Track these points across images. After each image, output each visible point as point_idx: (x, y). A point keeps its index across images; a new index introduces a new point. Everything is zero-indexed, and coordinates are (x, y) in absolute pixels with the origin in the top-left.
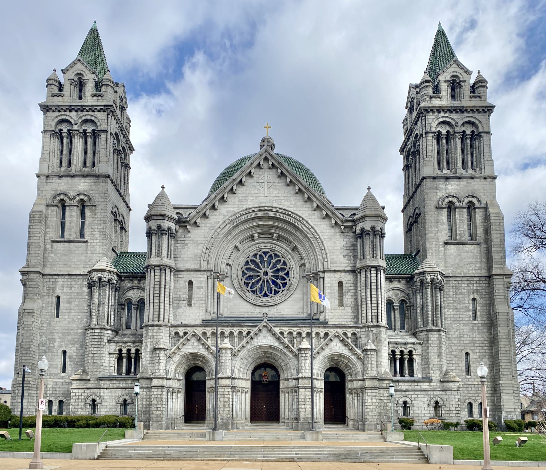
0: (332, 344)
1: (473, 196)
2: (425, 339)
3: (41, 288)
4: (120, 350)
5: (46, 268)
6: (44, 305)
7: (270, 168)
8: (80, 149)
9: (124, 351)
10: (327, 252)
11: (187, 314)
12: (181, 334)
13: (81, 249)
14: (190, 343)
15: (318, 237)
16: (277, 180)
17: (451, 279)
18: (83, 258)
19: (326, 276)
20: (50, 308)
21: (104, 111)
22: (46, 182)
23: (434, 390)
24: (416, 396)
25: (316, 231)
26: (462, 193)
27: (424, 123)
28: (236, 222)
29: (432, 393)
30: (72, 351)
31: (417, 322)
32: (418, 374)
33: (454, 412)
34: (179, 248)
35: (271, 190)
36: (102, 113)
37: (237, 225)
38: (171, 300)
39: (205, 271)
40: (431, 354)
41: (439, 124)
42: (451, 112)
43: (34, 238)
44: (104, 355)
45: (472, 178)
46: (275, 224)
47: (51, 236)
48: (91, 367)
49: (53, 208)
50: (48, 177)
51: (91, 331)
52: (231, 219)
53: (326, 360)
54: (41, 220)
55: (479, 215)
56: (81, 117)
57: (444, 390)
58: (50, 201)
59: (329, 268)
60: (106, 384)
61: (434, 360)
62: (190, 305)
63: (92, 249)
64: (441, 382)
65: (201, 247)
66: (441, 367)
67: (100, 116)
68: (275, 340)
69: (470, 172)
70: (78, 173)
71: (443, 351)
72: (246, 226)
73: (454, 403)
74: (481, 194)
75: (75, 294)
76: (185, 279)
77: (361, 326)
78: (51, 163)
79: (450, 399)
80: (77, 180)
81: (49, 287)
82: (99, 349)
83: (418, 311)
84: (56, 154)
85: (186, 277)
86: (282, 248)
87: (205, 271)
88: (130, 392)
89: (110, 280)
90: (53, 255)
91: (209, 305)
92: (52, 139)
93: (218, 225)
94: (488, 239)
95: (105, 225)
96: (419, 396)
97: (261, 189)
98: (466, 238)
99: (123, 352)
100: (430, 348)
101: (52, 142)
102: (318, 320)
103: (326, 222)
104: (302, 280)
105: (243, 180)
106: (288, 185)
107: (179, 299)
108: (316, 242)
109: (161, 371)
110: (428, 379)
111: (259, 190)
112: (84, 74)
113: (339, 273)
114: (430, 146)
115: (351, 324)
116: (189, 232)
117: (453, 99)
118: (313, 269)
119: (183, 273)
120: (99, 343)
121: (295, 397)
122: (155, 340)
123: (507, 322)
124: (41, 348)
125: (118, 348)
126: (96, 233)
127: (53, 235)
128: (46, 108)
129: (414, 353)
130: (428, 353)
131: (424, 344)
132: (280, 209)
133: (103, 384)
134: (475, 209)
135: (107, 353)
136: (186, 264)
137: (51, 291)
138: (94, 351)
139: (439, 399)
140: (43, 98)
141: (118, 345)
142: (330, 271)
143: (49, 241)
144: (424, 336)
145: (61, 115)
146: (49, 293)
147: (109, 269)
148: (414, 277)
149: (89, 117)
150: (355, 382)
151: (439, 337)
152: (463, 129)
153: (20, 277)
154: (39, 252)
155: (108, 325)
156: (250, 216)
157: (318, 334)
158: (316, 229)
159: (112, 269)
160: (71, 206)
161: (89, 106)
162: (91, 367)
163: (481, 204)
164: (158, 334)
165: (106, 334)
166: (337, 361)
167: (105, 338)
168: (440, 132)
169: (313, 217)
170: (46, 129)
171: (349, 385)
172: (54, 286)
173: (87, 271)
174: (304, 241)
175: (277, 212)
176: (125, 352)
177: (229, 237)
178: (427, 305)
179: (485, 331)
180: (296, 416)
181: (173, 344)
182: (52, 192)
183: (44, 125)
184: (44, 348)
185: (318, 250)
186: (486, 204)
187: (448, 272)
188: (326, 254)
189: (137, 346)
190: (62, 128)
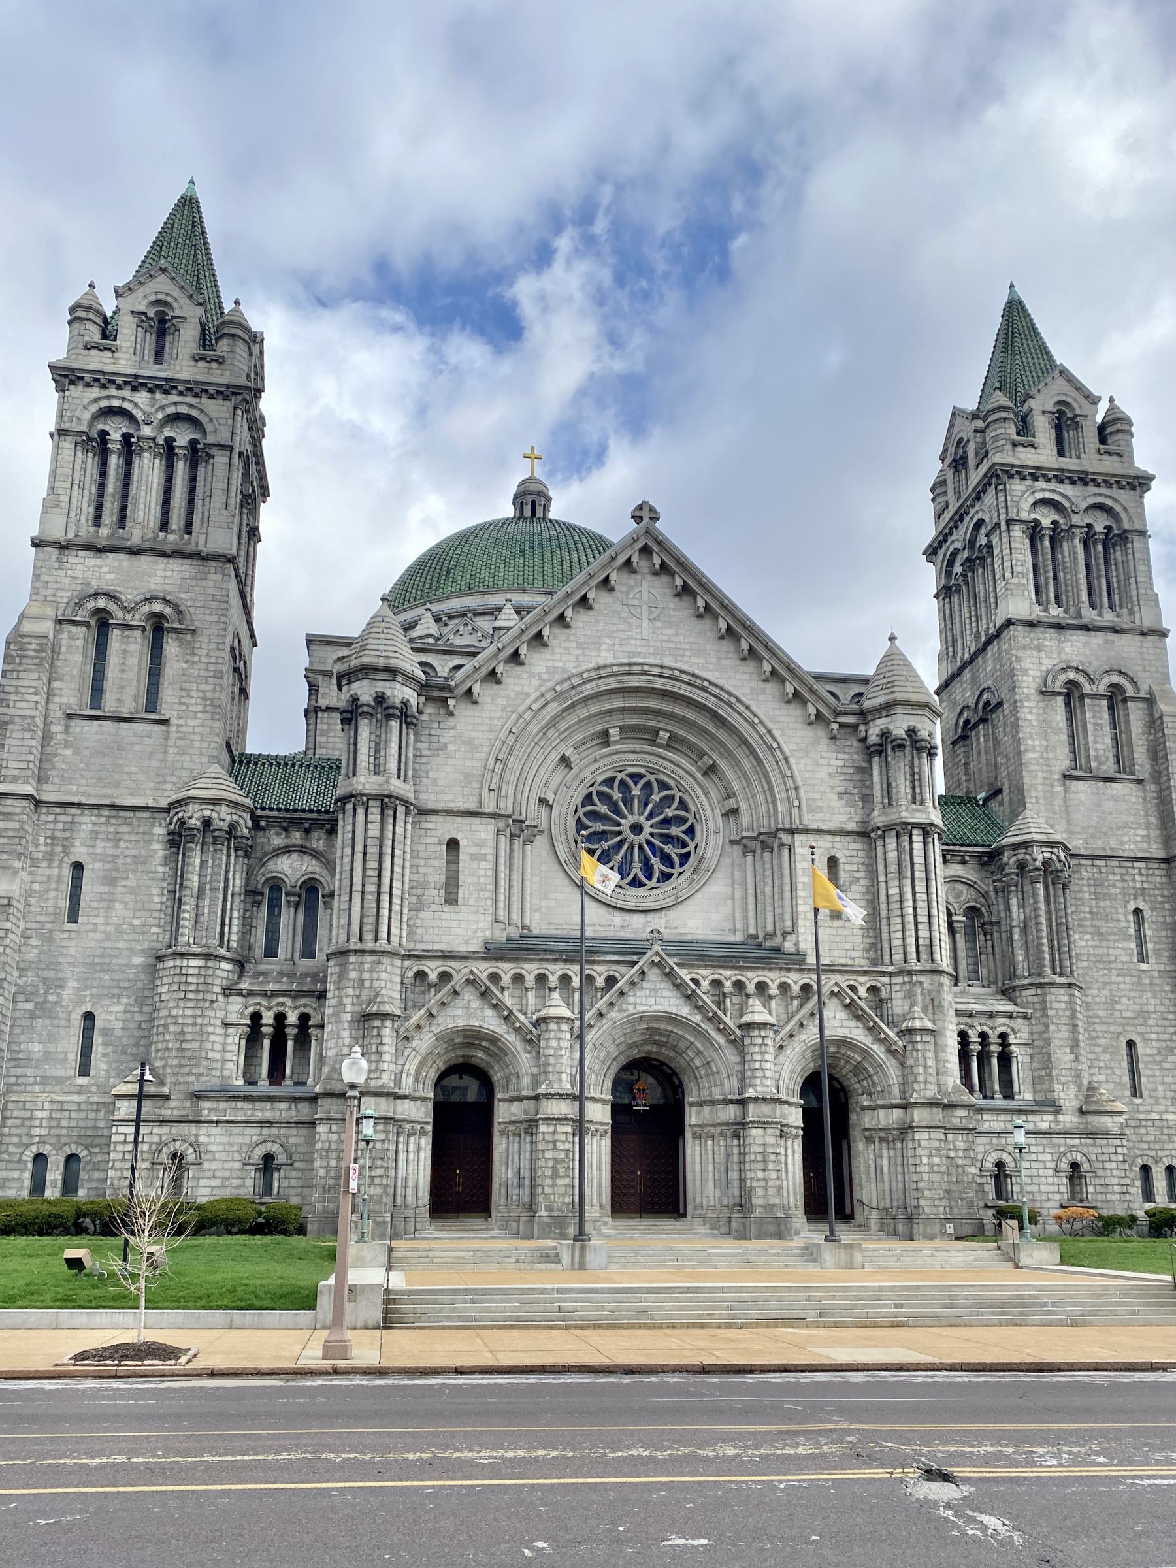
1: (1121, 672)
2: (1038, 1006)
3: (30, 838)
4: (256, 1017)
5: (45, 787)
6: (36, 887)
7: (655, 574)
8: (155, 486)
9: (268, 1018)
10: (800, 783)
12: (433, 977)
13: (150, 741)
14: (459, 1002)
15: (775, 745)
16: (673, 603)
17: (1083, 862)
18: (155, 764)
20: (52, 894)
21: (226, 398)
22: (59, 560)
25: (769, 732)
26: (1095, 663)
27: (1002, 499)
28: (571, 697)
30: (111, 1016)
31: (1013, 965)
32: (1024, 1094)
34: (425, 752)
35: (658, 624)
36: (220, 402)
38: (406, 886)
39: (494, 815)
40: (1055, 1043)
41: (1035, 504)
42: (1061, 482)
43: (19, 705)
44: (210, 1029)
45: (1115, 631)
46: (666, 707)
47: (65, 700)
48: (175, 1062)
49: (74, 629)
50: (64, 547)
51: (178, 962)
52: (558, 688)
53: (809, 1054)
54: (42, 659)
55: (1136, 715)
56: (162, 408)
58: (69, 611)
59: (805, 822)
60: (216, 1110)
61: (1062, 1057)
62: (451, 900)
63: (181, 743)
65: (484, 756)
67: (215, 410)
68: (681, 1001)
69: (1109, 617)
70: (147, 545)
72: (595, 708)
74: (1137, 668)
75: (129, 860)
76: (439, 833)
77: (891, 969)
78: (72, 514)
80: (144, 560)
81: (53, 838)
82: (199, 1012)
83: (1016, 937)
84: (86, 492)
85: (440, 829)
86: (678, 769)
87: (494, 815)
88: (283, 1131)
89: (233, 826)
90: (68, 752)
91: (501, 904)
92: (79, 454)
93: (528, 702)
94: (1160, 772)
95: (218, 681)
97: (634, 621)
98: (1109, 767)
99: (264, 1021)
100: (1052, 1027)
101: (79, 461)
102: (778, 950)
103: (794, 711)
104: (728, 848)
105: (591, 596)
106: (700, 616)
107: (423, 885)
108: (771, 758)
109: (385, 1076)
111: (630, 624)
112: (175, 305)
113: (829, 837)
114: (1015, 555)
115: (864, 964)
116: (451, 714)
117: (1061, 453)
118: (764, 825)
119: (433, 818)
120: (200, 996)
121: (735, 1151)
122: (366, 992)
124: (20, 1006)
125: (251, 1009)
126: (193, 701)
127: (72, 700)
129: (1012, 1039)
130: (1048, 1042)
131: (1037, 1016)
132: (682, 672)
133: (207, 1109)
134: (1125, 700)
135: (218, 1022)
136: (440, 796)
137: (59, 849)
138: (184, 1016)
140: (59, 352)
141: (252, 1001)
142: (807, 831)
143: (59, 714)
144: (1035, 999)
145: (109, 397)
146: (52, 854)
147: (233, 797)
148: (1002, 853)
149: (183, 410)
150: (882, 1112)
152: (1088, 520)
154: (33, 743)
155: (221, 945)
156: (606, 684)
157: (784, 987)
158: (770, 725)
159: (240, 799)
160: (125, 627)
161: (189, 382)
162: (175, 1062)
163: (1138, 690)
164: (375, 975)
165: (218, 972)
166: (832, 1056)
167: (218, 981)
168: (1037, 522)
169: (761, 697)
170: (66, 426)
171: (866, 1120)
172: (68, 834)
173: (170, 800)
174: (740, 753)
175: (675, 679)
176: (271, 1021)
178: (1038, 924)
179: (1168, 988)
180: (738, 1200)
181: (410, 1004)
182: (74, 587)
183: (60, 416)
184: (29, 1006)
185: (774, 777)
186: (1150, 692)
187: (1077, 844)
188: (797, 788)
189: (305, 1006)
190: (107, 428)
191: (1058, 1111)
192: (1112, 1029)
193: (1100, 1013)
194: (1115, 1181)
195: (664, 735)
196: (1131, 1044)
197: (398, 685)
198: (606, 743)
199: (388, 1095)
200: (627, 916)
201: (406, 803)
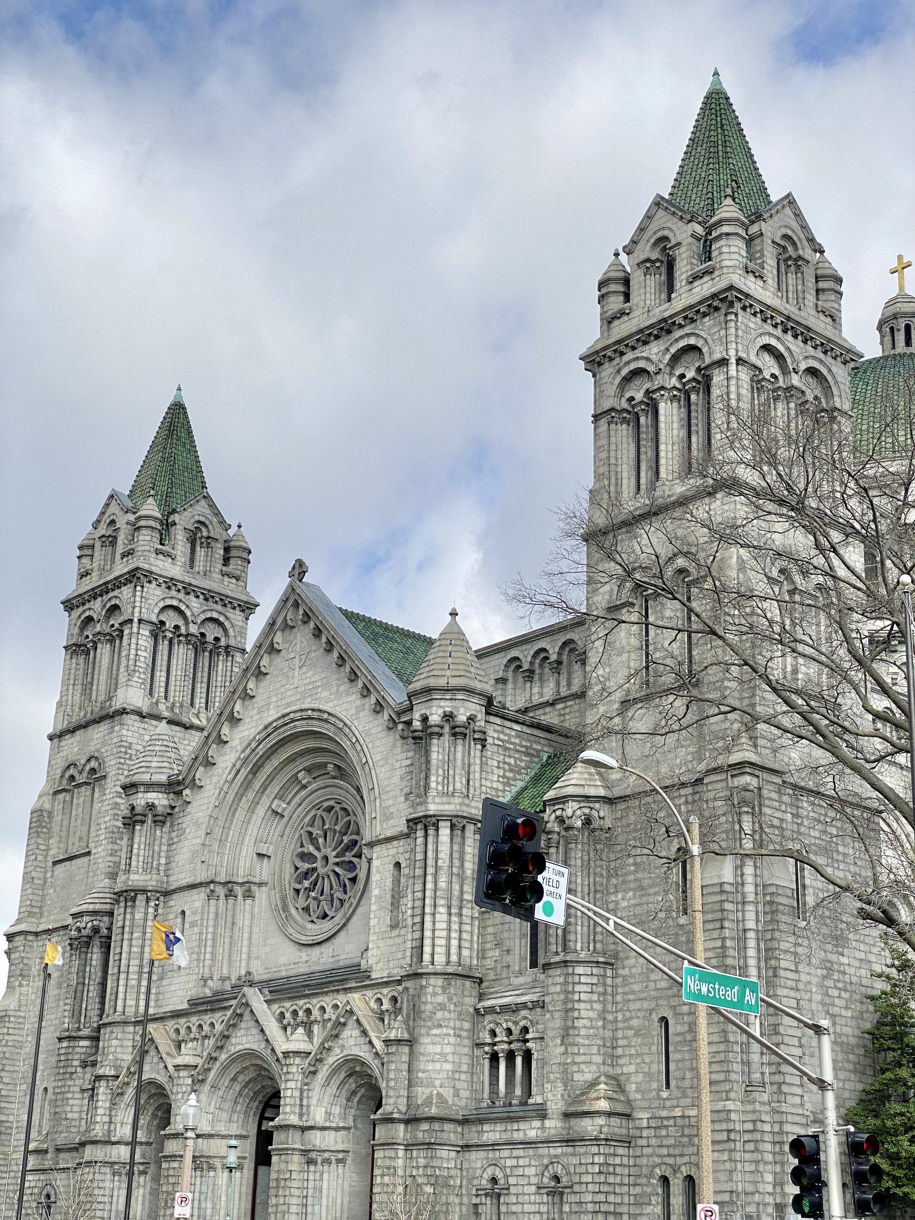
5: (43, 920)
11: (173, 988)
19: (375, 856)
29: (546, 1151)
35: (304, 669)
37: (256, 770)
39: (201, 884)
57: (568, 1141)
66: (565, 1072)
71: (579, 1023)
72: (276, 761)
73: (589, 1178)
79: (583, 1169)
85: (178, 902)
89: (96, 930)
97: (290, 674)
119: (175, 896)
132: (313, 710)
139: (559, 1170)
142: (380, 842)
151: (566, 982)
153: (5, 945)
167: (77, 1057)
175: (310, 718)
177: (251, 795)
192: (646, 1005)
193: (636, 987)
195: (330, 767)
196: (664, 1021)
197: (140, 795)
198: (304, 787)
200: (309, 951)
201: (145, 891)
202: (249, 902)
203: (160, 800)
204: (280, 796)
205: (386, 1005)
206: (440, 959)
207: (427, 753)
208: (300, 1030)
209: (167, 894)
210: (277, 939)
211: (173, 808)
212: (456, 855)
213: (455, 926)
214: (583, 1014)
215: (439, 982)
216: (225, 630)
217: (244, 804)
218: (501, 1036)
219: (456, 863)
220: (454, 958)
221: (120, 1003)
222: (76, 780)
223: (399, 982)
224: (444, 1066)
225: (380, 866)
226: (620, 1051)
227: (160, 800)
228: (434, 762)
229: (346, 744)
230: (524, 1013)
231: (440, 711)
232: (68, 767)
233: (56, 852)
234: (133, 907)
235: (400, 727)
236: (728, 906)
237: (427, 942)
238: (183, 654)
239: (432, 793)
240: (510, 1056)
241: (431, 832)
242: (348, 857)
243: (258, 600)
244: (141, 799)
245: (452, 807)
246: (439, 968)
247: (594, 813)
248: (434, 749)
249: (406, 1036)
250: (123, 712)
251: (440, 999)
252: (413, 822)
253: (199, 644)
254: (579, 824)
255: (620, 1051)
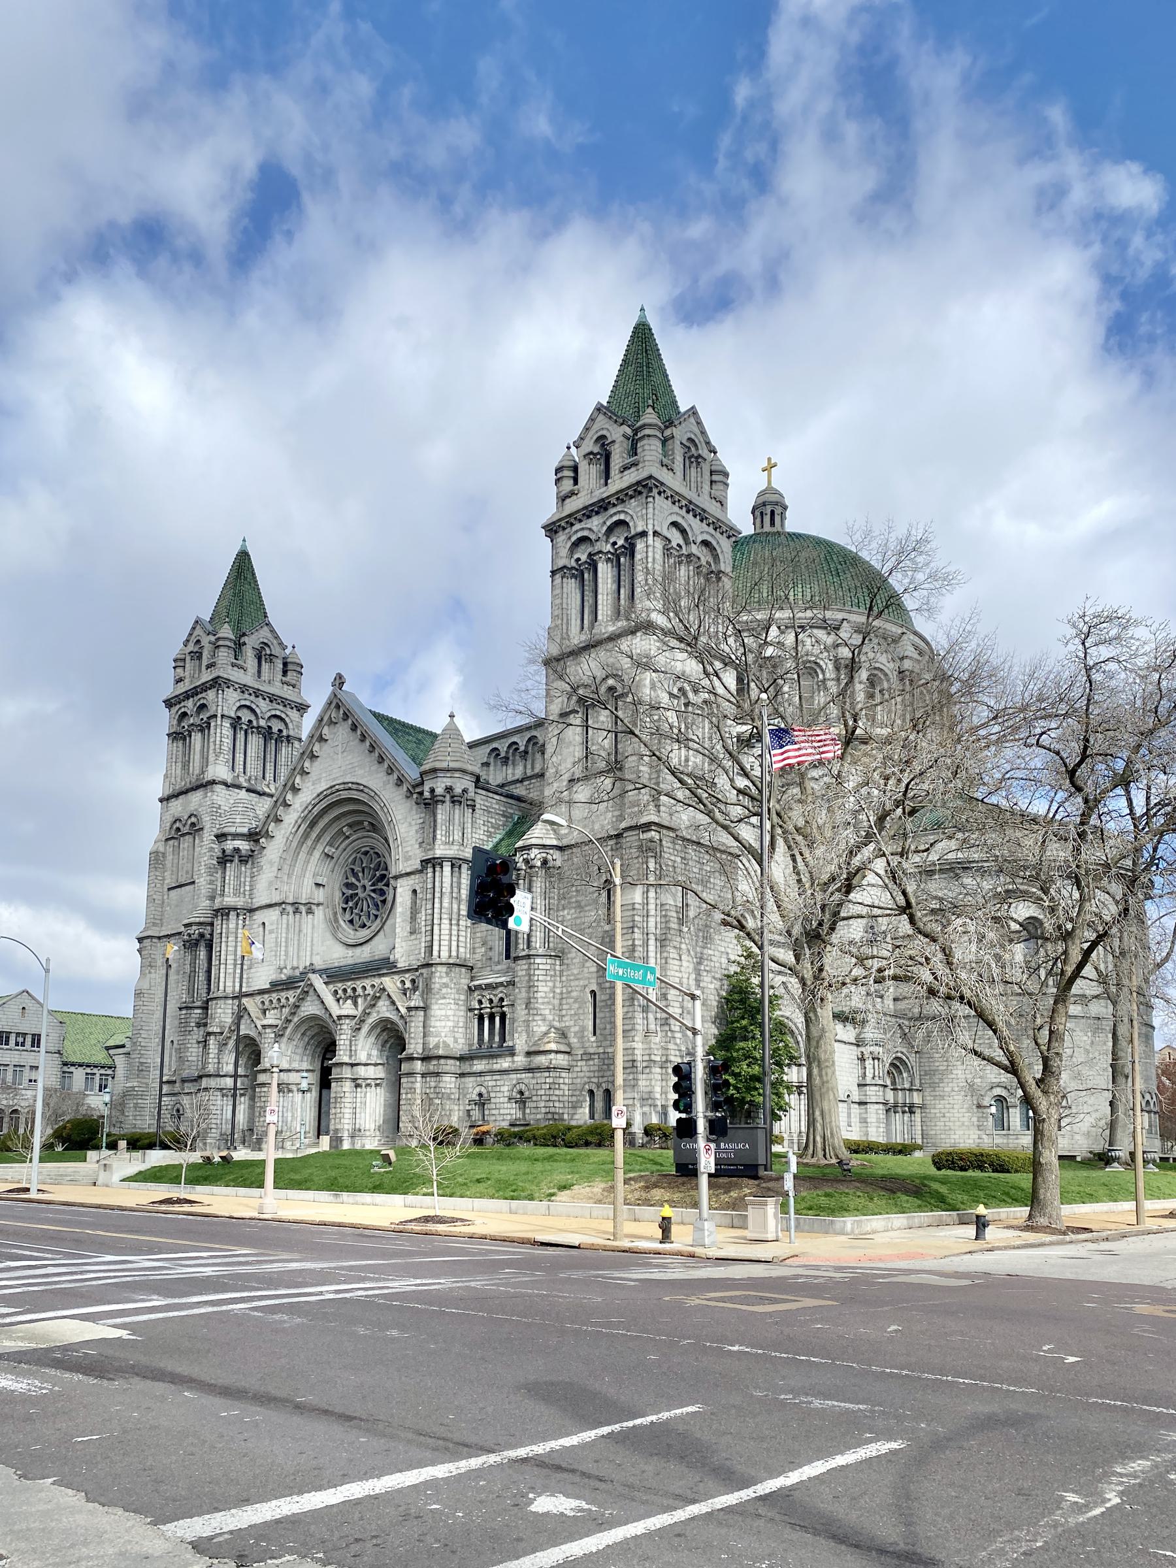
0: (380, 1003)
23: (516, 1071)
24: (494, 1083)
33: (543, 1110)
37: (312, 825)
39: (275, 905)
64: (529, 1054)
85: (259, 917)
89: (202, 935)
96: (498, 1083)
110: (512, 1052)
123: (631, 924)
128: (169, 703)
153: (138, 946)
175: (350, 789)
177: (309, 842)
191: (513, 1055)
192: (582, 983)
194: (542, 1104)
195: (366, 824)
198: (348, 837)
199: (210, 1076)
202: (310, 916)
203: (244, 846)
204: (330, 844)
205: (408, 985)
206: (444, 954)
207: (435, 815)
208: (349, 1001)
209: (252, 911)
210: (331, 942)
211: (253, 851)
212: (455, 885)
213: (454, 933)
214: (540, 989)
215: (443, 969)
216: (286, 724)
217: (305, 848)
218: (486, 1004)
219: (455, 890)
220: (454, 954)
221: (221, 984)
222: (183, 831)
223: (416, 970)
224: (447, 1024)
225: (403, 892)
226: (564, 1012)
227: (244, 846)
228: (439, 821)
229: (377, 808)
230: (501, 989)
231: (443, 786)
232: (175, 822)
233: (170, 881)
234: (228, 920)
235: (415, 796)
236: (637, 918)
237: (436, 943)
238: (255, 741)
239: (438, 842)
240: (492, 1017)
241: (438, 869)
242: (380, 886)
243: (309, 702)
244: (230, 845)
245: (452, 852)
246: (444, 961)
247: (549, 857)
248: (439, 811)
249: (422, 1005)
250: (213, 782)
251: (444, 980)
252: (425, 862)
253: (267, 734)
254: (539, 864)
255: (564, 1012)
